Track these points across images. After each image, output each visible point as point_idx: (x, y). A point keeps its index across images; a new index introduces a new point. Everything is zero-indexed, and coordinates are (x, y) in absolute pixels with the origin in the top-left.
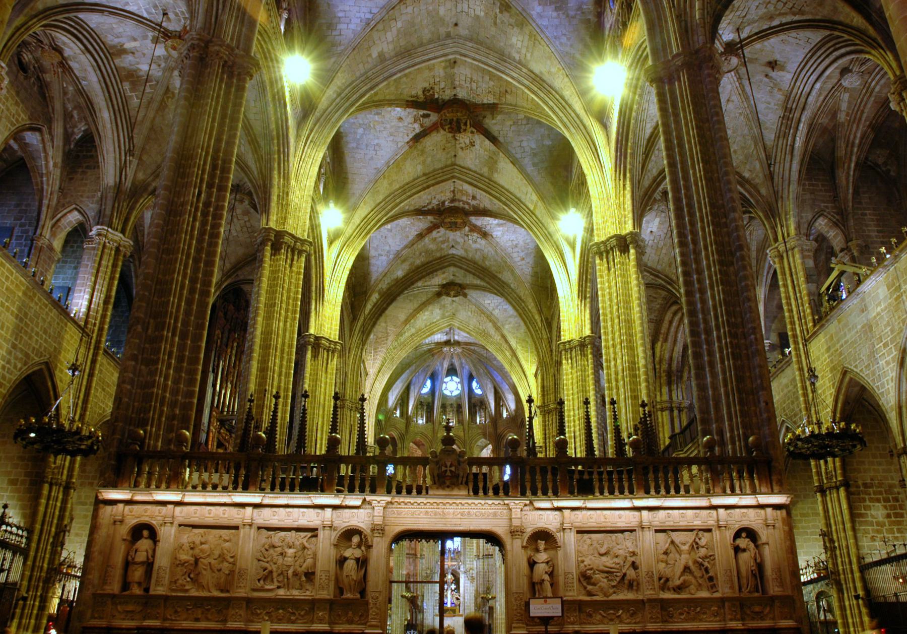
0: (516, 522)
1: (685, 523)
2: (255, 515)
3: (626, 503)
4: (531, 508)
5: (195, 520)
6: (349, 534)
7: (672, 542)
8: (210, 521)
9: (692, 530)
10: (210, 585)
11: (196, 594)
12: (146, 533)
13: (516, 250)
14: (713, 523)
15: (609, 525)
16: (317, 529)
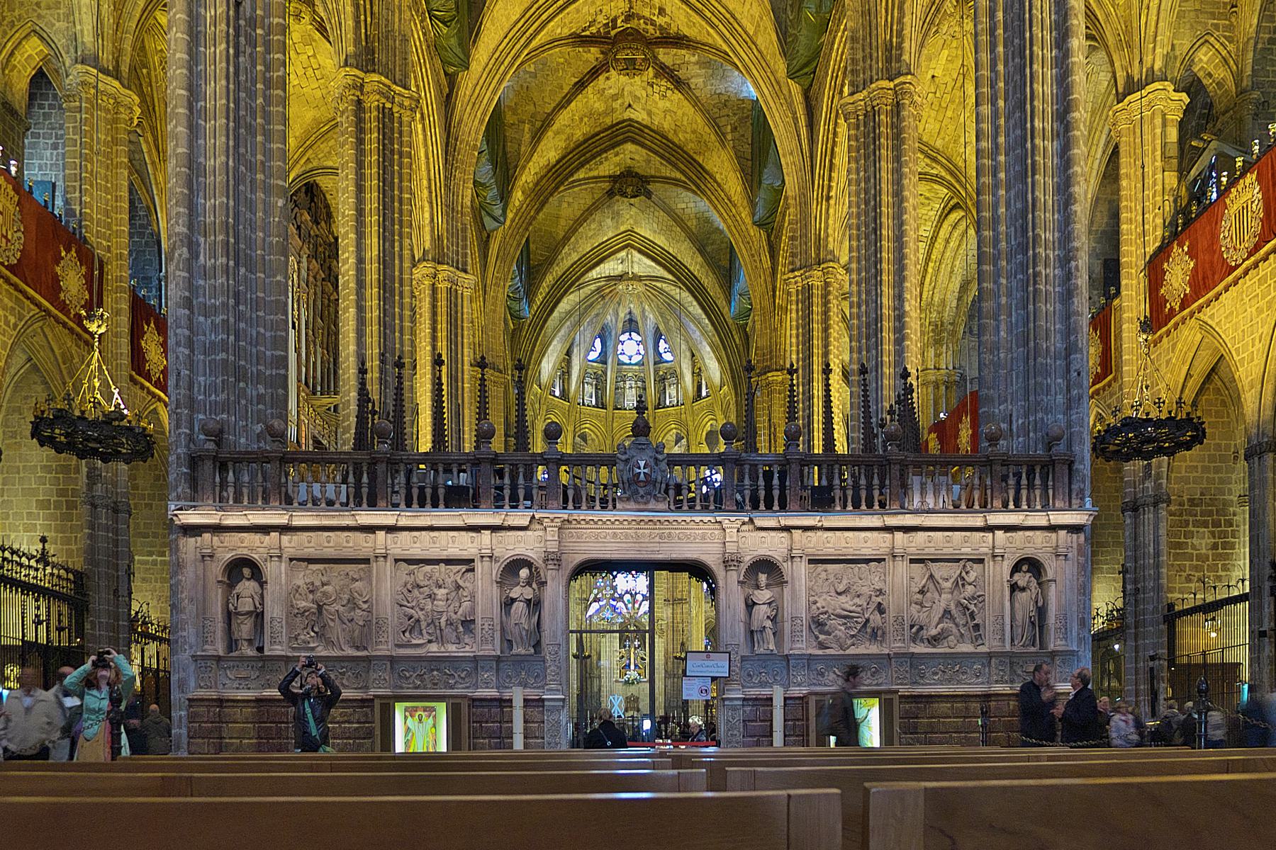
0: (731, 548)
1: (951, 551)
2: (389, 542)
3: (875, 521)
4: (751, 527)
5: (310, 552)
6: (515, 565)
7: (931, 576)
8: (329, 553)
9: (958, 560)
10: (342, 641)
11: (324, 653)
12: (246, 572)
13: (725, 111)
14: (986, 550)
15: (850, 553)
16: (473, 561)
